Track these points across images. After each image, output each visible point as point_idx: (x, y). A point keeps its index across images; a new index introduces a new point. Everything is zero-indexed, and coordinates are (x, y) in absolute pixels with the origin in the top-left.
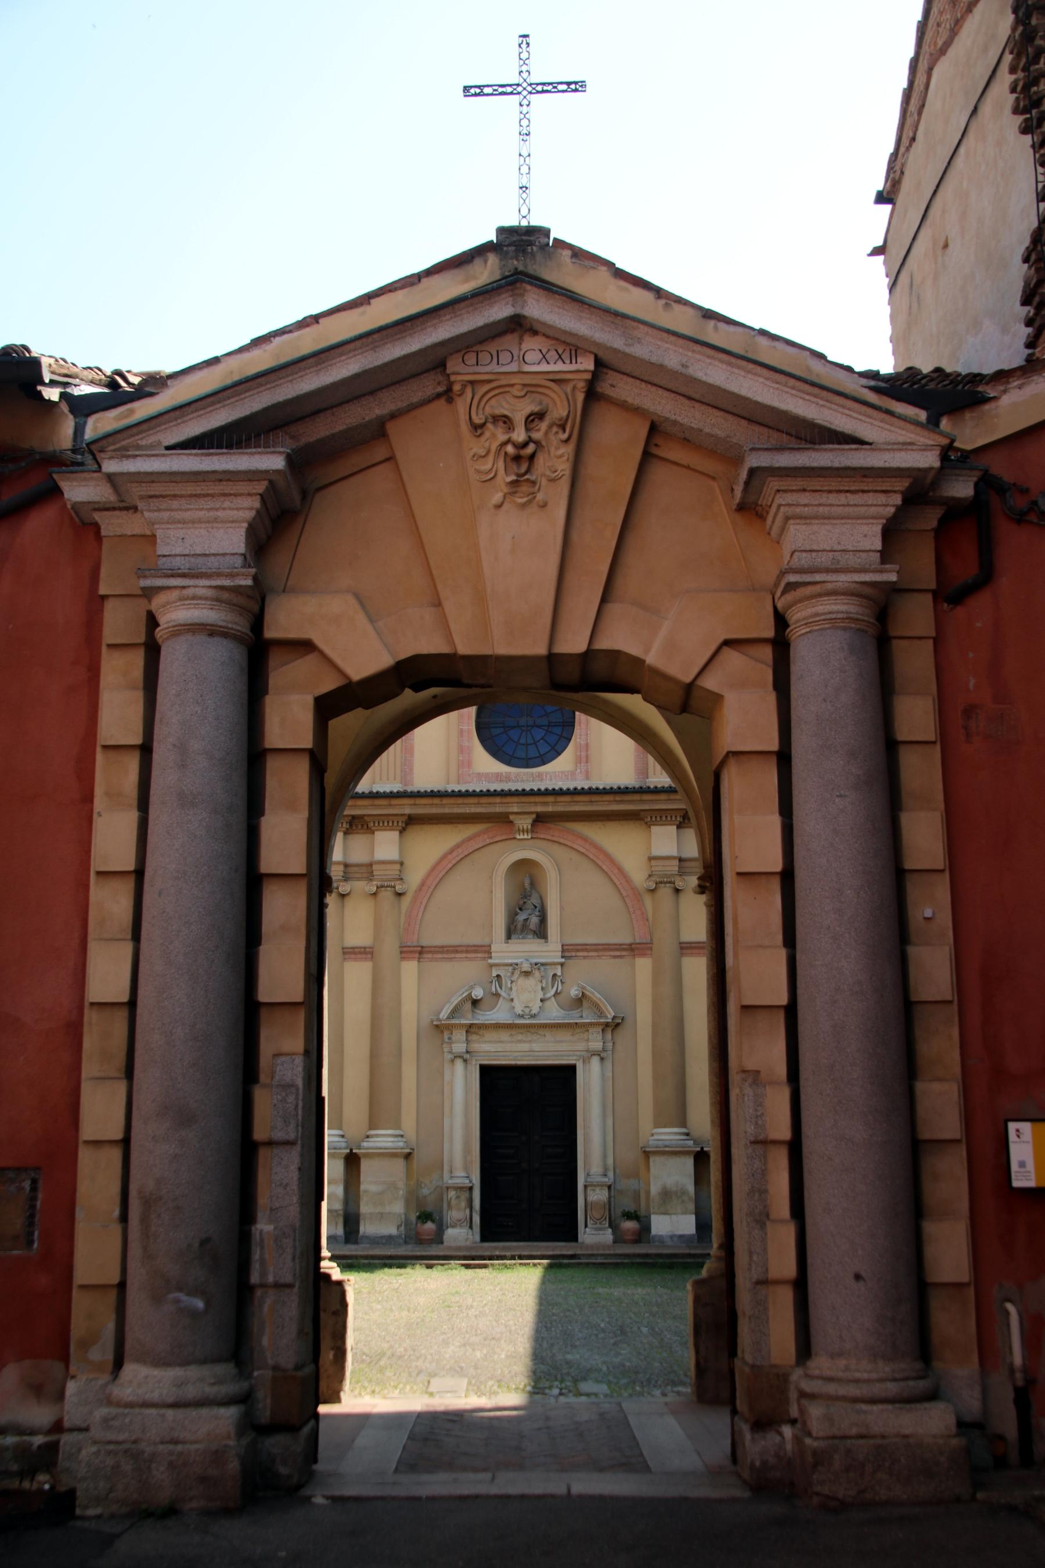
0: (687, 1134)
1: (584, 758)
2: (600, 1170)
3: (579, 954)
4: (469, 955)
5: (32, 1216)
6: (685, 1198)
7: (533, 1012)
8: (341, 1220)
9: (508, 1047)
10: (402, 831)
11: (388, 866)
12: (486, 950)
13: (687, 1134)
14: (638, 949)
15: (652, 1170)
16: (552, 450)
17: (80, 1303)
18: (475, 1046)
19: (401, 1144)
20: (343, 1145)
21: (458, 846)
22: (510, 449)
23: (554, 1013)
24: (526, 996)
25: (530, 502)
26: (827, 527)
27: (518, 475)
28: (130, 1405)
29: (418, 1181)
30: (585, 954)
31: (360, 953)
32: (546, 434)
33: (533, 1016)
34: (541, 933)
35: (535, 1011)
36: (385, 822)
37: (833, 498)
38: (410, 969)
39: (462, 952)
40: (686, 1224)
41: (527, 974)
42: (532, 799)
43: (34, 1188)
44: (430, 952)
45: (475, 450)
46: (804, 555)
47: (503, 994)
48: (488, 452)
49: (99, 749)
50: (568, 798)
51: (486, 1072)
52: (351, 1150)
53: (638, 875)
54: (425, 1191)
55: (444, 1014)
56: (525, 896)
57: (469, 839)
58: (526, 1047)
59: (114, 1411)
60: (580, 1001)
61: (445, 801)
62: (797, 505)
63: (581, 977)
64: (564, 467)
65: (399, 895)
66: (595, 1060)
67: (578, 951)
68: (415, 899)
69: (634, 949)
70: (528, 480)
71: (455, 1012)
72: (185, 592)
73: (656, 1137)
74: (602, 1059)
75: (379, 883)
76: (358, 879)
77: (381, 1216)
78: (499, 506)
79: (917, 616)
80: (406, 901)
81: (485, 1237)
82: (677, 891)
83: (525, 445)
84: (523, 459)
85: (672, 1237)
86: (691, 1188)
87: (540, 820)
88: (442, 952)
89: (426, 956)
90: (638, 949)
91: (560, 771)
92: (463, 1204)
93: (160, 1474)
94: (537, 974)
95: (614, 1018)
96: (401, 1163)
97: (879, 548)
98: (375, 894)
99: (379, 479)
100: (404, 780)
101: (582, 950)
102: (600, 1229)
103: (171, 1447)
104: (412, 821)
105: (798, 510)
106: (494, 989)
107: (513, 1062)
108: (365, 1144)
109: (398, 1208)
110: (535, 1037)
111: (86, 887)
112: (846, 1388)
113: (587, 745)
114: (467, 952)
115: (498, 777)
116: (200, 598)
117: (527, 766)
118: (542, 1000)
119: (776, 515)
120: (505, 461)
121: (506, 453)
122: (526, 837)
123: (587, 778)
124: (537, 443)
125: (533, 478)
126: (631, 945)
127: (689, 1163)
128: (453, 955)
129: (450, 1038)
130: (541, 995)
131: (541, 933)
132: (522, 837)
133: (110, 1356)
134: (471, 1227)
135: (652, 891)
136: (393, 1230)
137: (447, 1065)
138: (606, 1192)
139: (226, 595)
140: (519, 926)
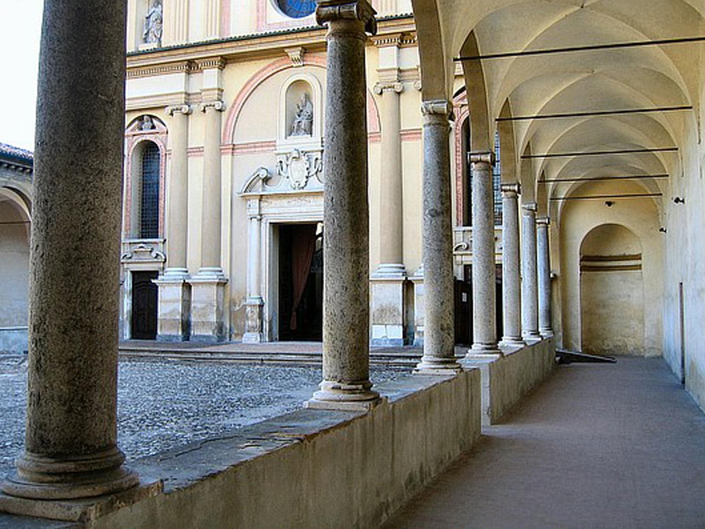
0: (403, 268)
6: (396, 313)
12: (272, 144)
33: (303, 188)
35: (302, 185)
39: (259, 147)
40: (397, 333)
57: (264, 69)
68: (230, 113)
71: (249, 187)
80: (224, 115)
89: (238, 151)
104: (225, 61)
122: (299, 64)
128: (253, 150)
132: (297, 65)
135: (381, 93)
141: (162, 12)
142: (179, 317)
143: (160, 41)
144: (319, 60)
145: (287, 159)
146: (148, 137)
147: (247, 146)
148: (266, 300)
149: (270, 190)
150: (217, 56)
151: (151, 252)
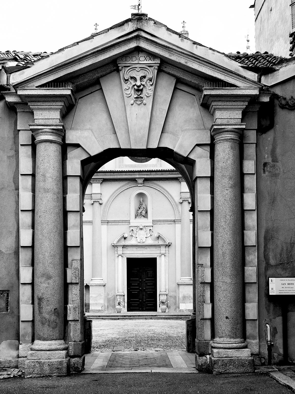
3: (157, 223)
4: (123, 223)
5: (8, 303)
6: (190, 298)
7: (143, 241)
9: (135, 252)
10: (101, 183)
12: (129, 222)
14: (176, 221)
15: (180, 290)
16: (148, 87)
17: (22, 325)
18: (125, 252)
19: (102, 282)
21: (119, 189)
22: (136, 87)
23: (150, 241)
24: (142, 237)
25: (141, 103)
26: (226, 111)
27: (138, 95)
28: (38, 350)
29: (108, 293)
30: (160, 223)
31: (88, 223)
32: (146, 83)
34: (146, 216)
37: (228, 103)
38: (105, 227)
42: (143, 173)
43: (8, 296)
44: (110, 222)
45: (126, 87)
46: (219, 120)
48: (129, 88)
49: (20, 175)
50: (154, 173)
51: (128, 259)
52: (87, 284)
53: (177, 199)
54: (110, 297)
55: (115, 242)
56: (141, 204)
58: (141, 252)
59: (33, 352)
60: (158, 237)
61: (115, 174)
62: (217, 105)
63: (159, 229)
64: (151, 93)
65: (101, 204)
67: (158, 222)
68: (105, 205)
70: (141, 97)
72: (43, 130)
73: (181, 280)
75: (94, 200)
77: (96, 304)
78: (132, 105)
79: (252, 136)
81: (128, 311)
83: (140, 86)
84: (139, 90)
85: (186, 310)
87: (146, 180)
88: (115, 222)
89: (109, 224)
90: (176, 221)
93: (46, 368)
94: (144, 229)
97: (241, 118)
98: (93, 204)
99: (97, 95)
101: (159, 222)
103: (49, 360)
105: (218, 107)
106: (131, 234)
107: (137, 257)
108: (91, 282)
109: (102, 301)
110: (144, 249)
111: (17, 215)
112: (225, 348)
115: (132, 166)
116: (47, 132)
117: (142, 162)
118: (146, 238)
119: (212, 108)
120: (134, 91)
121: (134, 88)
122: (141, 185)
124: (143, 85)
125: (142, 96)
126: (174, 220)
128: (118, 223)
129: (117, 250)
131: (146, 216)
132: (140, 185)
133: (30, 339)
135: (181, 203)
136: (100, 309)
139: (54, 131)
140: (139, 214)
144: (151, 184)
147: (115, 222)
149: (127, 243)
150: (102, 178)
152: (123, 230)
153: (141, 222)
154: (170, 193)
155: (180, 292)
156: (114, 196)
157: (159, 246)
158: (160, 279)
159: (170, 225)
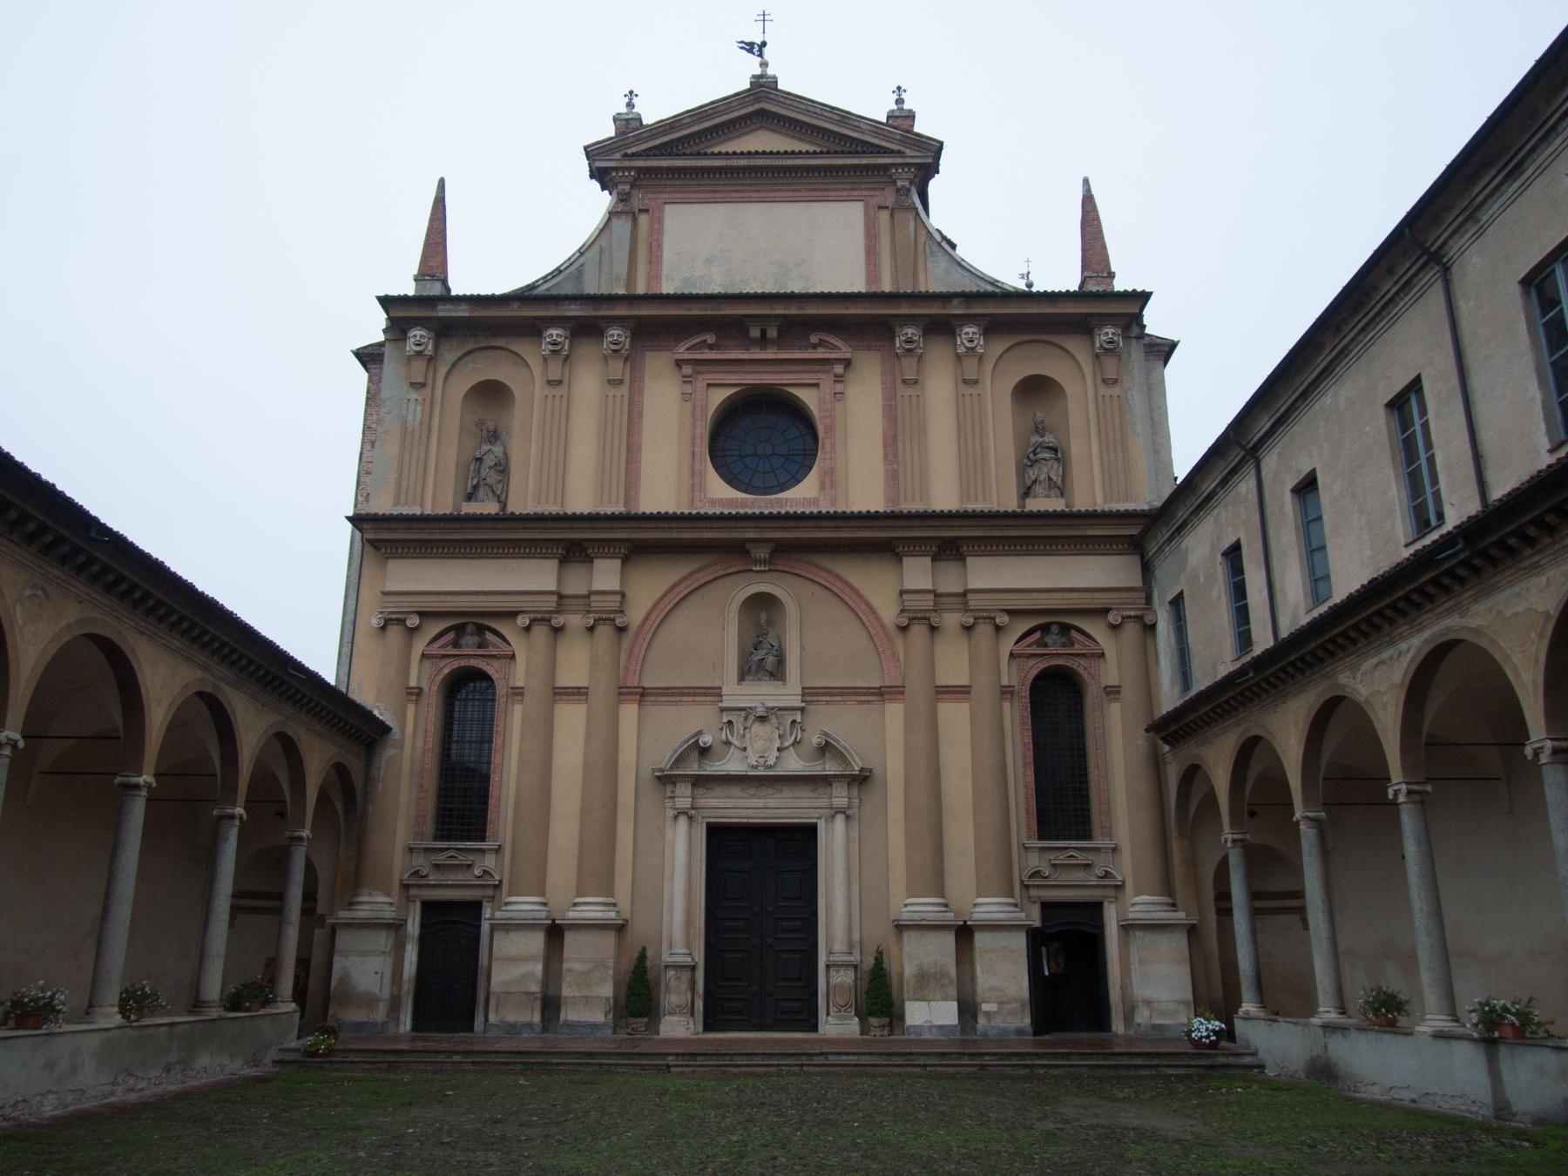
0: (946, 905)
1: (829, 482)
2: (845, 949)
6: (946, 981)
8: (538, 1004)
9: (740, 802)
10: (626, 560)
11: (609, 598)
12: (716, 692)
13: (946, 905)
15: (906, 948)
18: (702, 802)
19: (613, 915)
20: (543, 915)
23: (794, 764)
34: (777, 673)
35: (771, 762)
36: (606, 548)
41: (762, 719)
47: (735, 742)
53: (889, 613)
58: (760, 803)
65: (621, 630)
66: (840, 819)
68: (637, 634)
69: (883, 693)
71: (680, 760)
74: (848, 817)
76: (574, 612)
80: (627, 639)
81: (708, 1027)
82: (933, 629)
85: (930, 1028)
86: (953, 971)
88: (666, 695)
91: (804, 495)
92: (684, 986)
94: (774, 720)
95: (862, 770)
96: (609, 939)
98: (591, 629)
100: (626, 503)
102: (846, 1018)
108: (571, 914)
113: (832, 470)
114: (695, 695)
118: (779, 750)
123: (833, 504)
127: (949, 939)
130: (777, 744)
131: (777, 673)
134: (692, 1015)
135: (903, 629)
137: (669, 823)
138: (851, 974)
141: (505, 454)
142: (535, 988)
143: (504, 505)
145: (746, 719)
146: (472, 662)
148: (699, 957)
151: (469, 866)
152: (698, 720)
153: (761, 694)
154: (863, 592)
155: (905, 957)
156: (669, 606)
157: (824, 781)
158: (829, 907)
159: (866, 706)
